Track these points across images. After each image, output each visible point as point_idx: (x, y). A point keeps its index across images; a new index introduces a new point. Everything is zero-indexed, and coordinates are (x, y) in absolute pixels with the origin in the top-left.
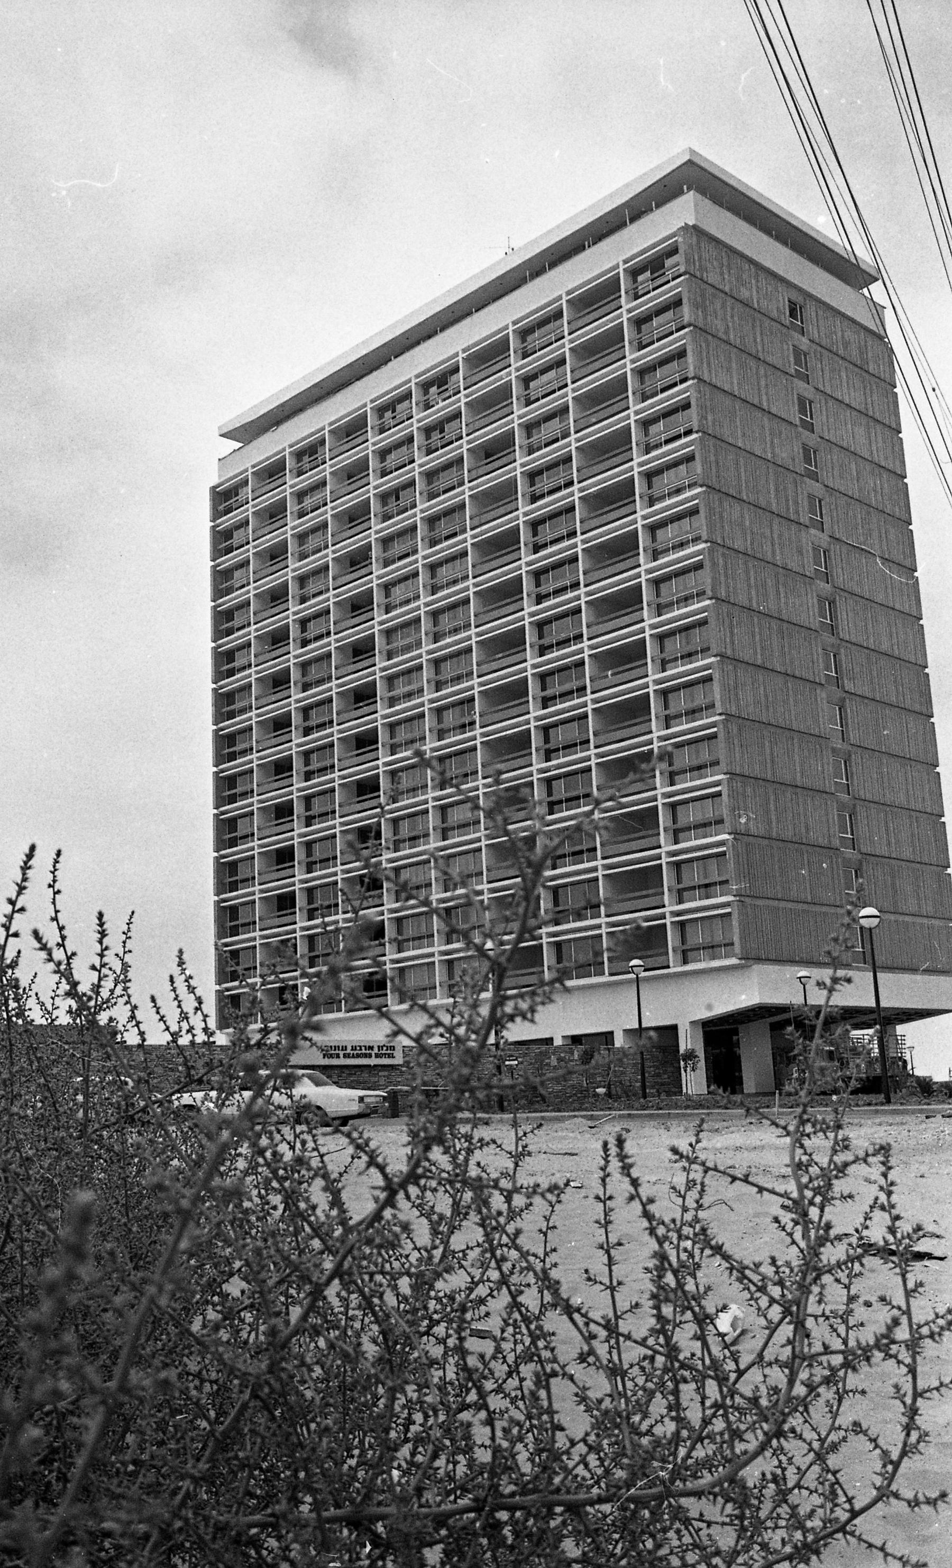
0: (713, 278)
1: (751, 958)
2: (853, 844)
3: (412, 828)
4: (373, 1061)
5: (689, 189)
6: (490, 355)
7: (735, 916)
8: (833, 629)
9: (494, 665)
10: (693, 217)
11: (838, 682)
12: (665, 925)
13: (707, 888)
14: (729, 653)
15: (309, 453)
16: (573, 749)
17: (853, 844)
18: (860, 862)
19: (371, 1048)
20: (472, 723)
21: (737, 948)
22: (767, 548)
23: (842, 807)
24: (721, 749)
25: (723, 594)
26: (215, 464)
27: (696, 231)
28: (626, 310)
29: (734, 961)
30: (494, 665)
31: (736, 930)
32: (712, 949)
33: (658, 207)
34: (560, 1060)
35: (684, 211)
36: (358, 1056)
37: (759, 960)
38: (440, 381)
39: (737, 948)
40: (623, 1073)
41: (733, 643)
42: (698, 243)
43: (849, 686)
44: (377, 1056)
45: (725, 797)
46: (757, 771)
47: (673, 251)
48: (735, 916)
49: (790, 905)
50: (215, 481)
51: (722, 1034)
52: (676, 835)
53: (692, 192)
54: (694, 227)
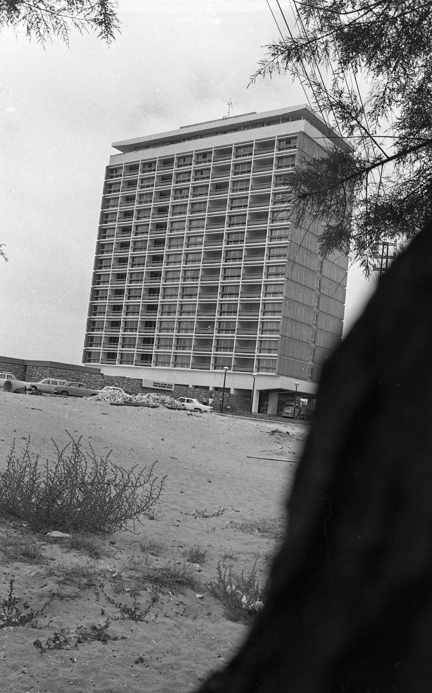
0: (306, 150)
1: (280, 374)
2: (314, 342)
3: (169, 308)
4: (166, 389)
5: (304, 119)
6: (224, 152)
7: (277, 361)
8: (321, 272)
9: (209, 261)
10: (304, 128)
11: (319, 290)
12: (254, 359)
13: (269, 350)
14: (290, 278)
15: (149, 165)
16: (232, 295)
17: (314, 342)
18: (315, 348)
19: (166, 385)
20: (197, 278)
21: (276, 370)
22: (306, 244)
23: (313, 330)
24: (282, 308)
25: (291, 258)
26: (109, 157)
27: (304, 134)
28: (275, 153)
29: (274, 374)
30: (209, 261)
31: (277, 365)
32: (267, 369)
33: (292, 121)
34: (216, 395)
35: (300, 125)
36: (162, 387)
37: (282, 375)
38: (204, 155)
39: (276, 370)
40: (232, 402)
41: (291, 275)
42: (303, 139)
43: (322, 291)
44: (167, 387)
45: (281, 323)
46: (291, 317)
47: (296, 138)
48: (277, 361)
49: (294, 359)
50: (108, 164)
51: (264, 395)
52: (262, 332)
53: (305, 120)
54: (303, 132)
